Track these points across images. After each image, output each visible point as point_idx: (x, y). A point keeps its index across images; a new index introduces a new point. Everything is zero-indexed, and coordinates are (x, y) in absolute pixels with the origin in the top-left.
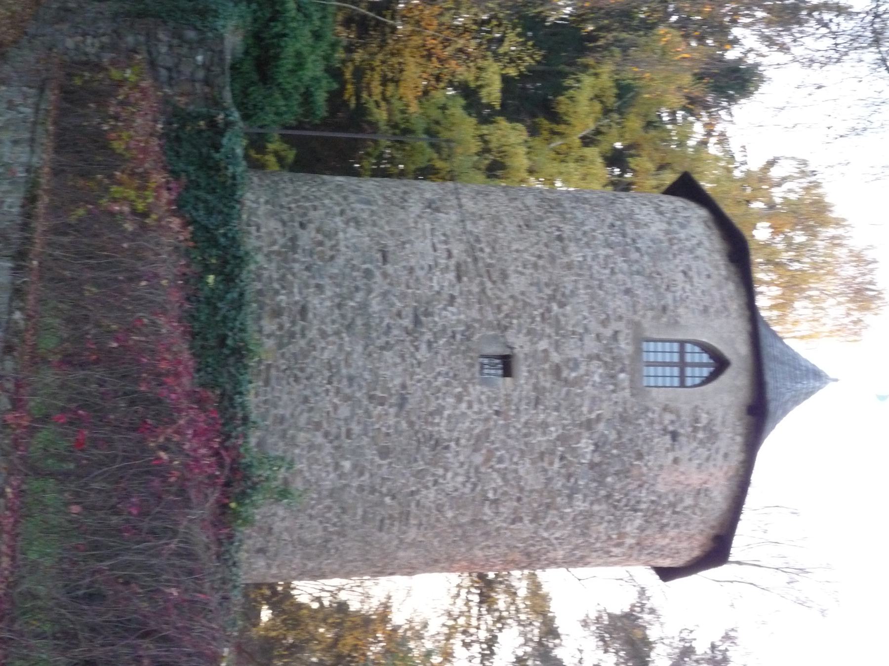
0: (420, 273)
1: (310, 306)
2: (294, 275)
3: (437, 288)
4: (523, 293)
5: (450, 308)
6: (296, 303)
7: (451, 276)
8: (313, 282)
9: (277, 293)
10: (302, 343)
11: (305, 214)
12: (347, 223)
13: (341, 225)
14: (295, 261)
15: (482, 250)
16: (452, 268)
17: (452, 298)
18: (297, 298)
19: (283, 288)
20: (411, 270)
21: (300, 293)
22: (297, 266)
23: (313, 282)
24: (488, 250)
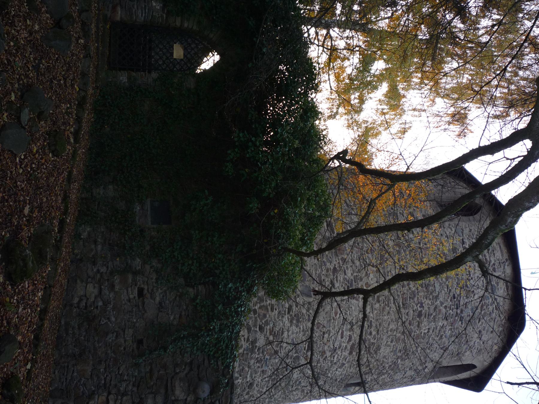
0: (328, 354)
1: (256, 382)
2: (249, 367)
3: (335, 361)
4: (384, 357)
5: (339, 370)
6: (247, 382)
7: (346, 353)
8: (260, 370)
9: (237, 378)
10: (246, 397)
11: (265, 316)
12: (291, 322)
13: (287, 324)
14: (251, 358)
15: (371, 334)
16: (349, 348)
17: (343, 364)
18: (248, 380)
19: (241, 376)
20: (324, 352)
21: (251, 376)
22: (252, 362)
23: (260, 370)
24: (374, 333)
